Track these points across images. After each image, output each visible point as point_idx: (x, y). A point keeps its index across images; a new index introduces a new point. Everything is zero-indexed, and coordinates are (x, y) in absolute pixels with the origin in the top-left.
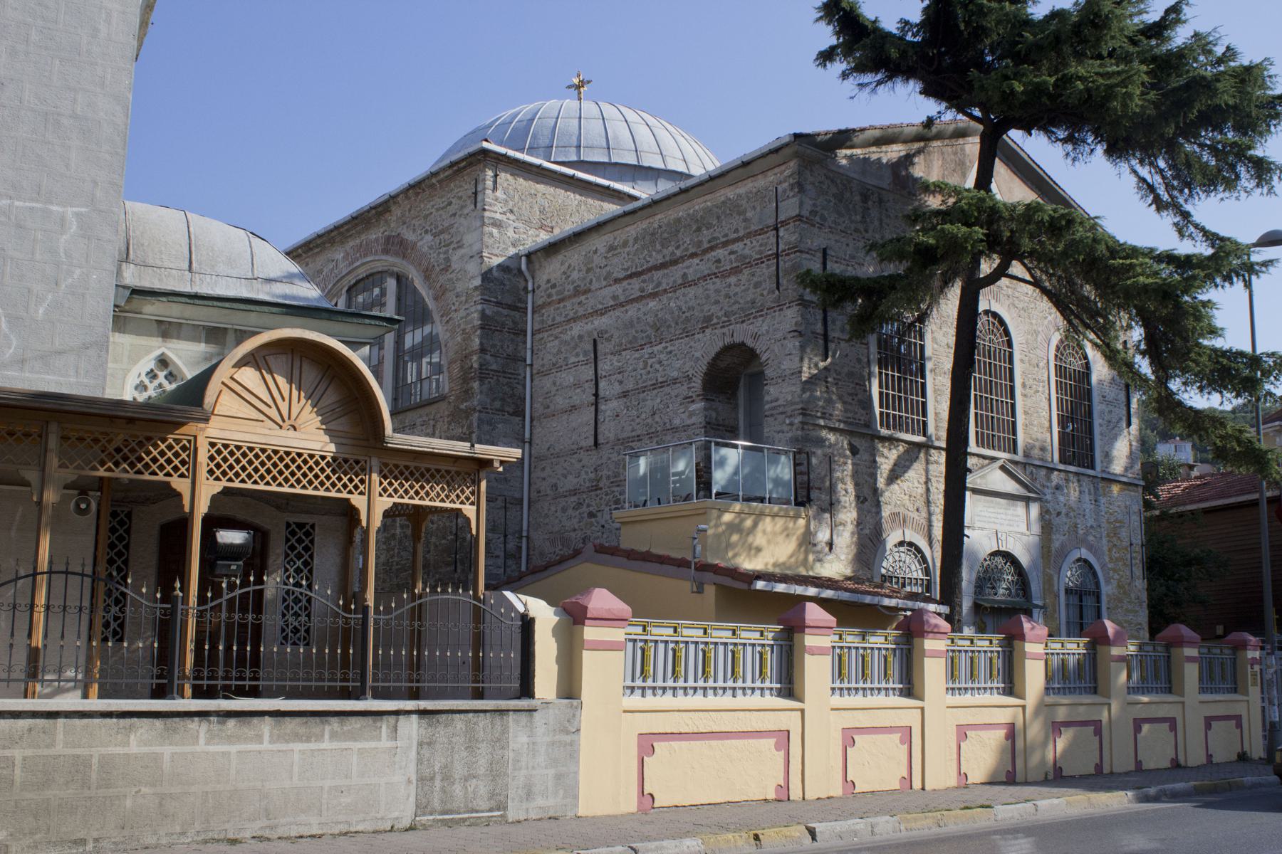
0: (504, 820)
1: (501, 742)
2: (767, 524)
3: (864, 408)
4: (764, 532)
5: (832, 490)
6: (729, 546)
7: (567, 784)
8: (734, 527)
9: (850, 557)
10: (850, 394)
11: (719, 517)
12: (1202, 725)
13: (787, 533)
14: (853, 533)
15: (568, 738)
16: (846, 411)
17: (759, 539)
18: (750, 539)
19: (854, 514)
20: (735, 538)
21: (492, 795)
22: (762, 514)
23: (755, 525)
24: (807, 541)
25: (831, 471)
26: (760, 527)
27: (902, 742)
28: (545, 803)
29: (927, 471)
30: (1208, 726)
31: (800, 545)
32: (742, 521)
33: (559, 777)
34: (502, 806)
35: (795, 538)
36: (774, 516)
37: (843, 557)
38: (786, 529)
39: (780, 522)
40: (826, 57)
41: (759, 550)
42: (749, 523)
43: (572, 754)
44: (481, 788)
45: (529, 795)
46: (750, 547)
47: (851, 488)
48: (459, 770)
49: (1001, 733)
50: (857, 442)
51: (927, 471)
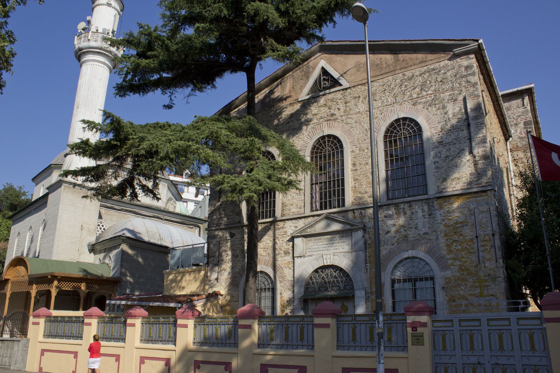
0: (10, 369)
1: (12, 349)
2: (187, 277)
3: (238, 215)
4: (186, 280)
5: (220, 255)
6: (172, 288)
7: (24, 360)
8: (173, 281)
9: (228, 283)
10: (231, 211)
11: (168, 277)
12: (39, 352)
13: (195, 279)
14: (229, 273)
15: (25, 349)
16: (228, 219)
17: (184, 284)
18: (180, 284)
19: (230, 264)
20: (173, 285)
21: (9, 362)
22: (184, 273)
23: (182, 278)
24: (205, 280)
25: (219, 248)
26: (184, 279)
27: (116, 361)
28: (19, 366)
29: (274, 234)
30: (42, 354)
31: (201, 283)
32: (177, 277)
33: (23, 359)
34: (10, 366)
35: (199, 281)
36: (190, 273)
37: (224, 284)
38: (195, 278)
39: (192, 275)
40: (114, 87)
41: (184, 288)
42: (179, 278)
43: (26, 354)
44: (7, 359)
45: (16, 363)
46: (180, 287)
47: (230, 253)
48: (5, 355)
49: (163, 363)
50: (233, 231)
51: (274, 234)
